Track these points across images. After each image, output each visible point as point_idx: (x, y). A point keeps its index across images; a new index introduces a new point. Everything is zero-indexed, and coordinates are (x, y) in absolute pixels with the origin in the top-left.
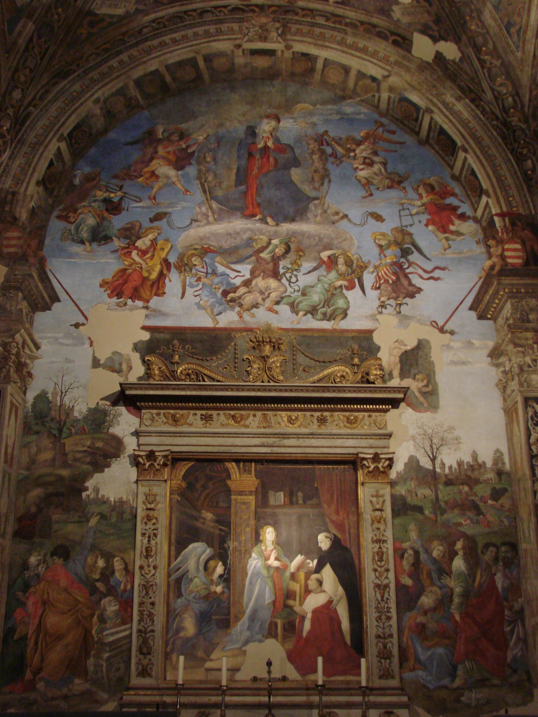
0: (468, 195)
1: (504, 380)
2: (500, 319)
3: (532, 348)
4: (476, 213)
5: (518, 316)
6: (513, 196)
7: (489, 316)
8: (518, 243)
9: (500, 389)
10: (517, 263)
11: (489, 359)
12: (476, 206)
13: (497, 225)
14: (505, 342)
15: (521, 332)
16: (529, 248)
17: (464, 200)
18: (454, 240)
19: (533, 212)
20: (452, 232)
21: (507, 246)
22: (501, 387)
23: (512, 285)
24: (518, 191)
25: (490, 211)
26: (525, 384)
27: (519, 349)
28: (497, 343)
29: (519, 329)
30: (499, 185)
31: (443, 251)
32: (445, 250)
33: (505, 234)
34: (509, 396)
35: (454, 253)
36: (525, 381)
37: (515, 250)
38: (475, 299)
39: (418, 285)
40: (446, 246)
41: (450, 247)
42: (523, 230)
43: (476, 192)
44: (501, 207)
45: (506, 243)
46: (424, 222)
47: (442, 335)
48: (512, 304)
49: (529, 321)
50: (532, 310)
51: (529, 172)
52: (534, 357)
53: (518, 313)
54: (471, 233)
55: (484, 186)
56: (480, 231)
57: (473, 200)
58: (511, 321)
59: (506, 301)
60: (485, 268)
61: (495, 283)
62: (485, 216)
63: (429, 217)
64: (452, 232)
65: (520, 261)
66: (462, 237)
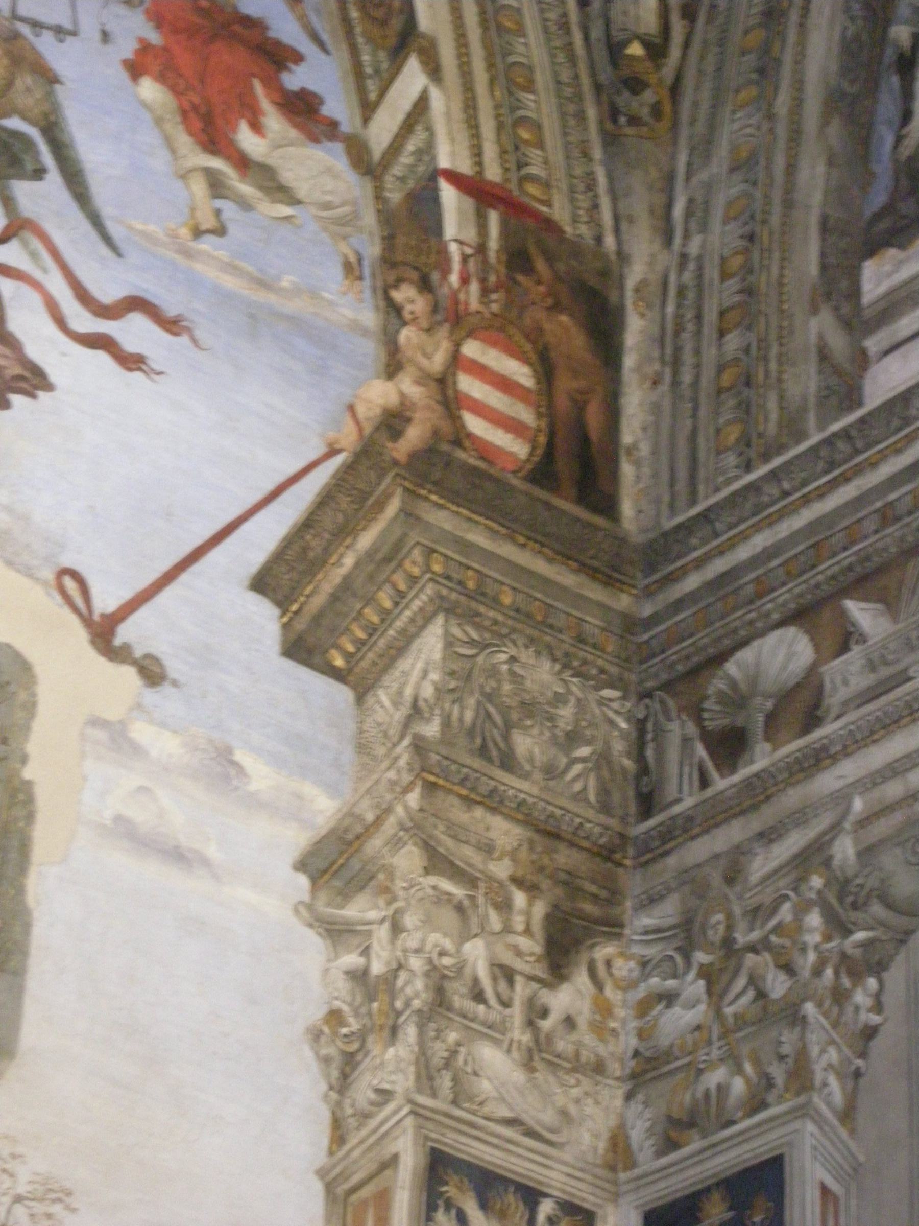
0: (346, 20)
1: (354, 1025)
2: (383, 696)
3: (504, 906)
4: (366, 120)
5: (469, 715)
6: (537, 127)
7: (339, 662)
8: (523, 358)
9: (326, 1060)
10: (499, 451)
11: (303, 881)
12: (372, 87)
13: (450, 230)
14: (390, 826)
15: (469, 802)
16: (562, 402)
17: (325, 37)
18: (245, 205)
19: (610, 241)
20: (243, 163)
21: (472, 349)
22: (331, 1051)
23: (466, 547)
24: (563, 115)
25: (428, 149)
26: (445, 1082)
27: (446, 885)
28: (351, 814)
29: (463, 782)
30: (487, 45)
31: (185, 232)
32: (198, 233)
33: (474, 287)
34: (367, 1116)
35: (230, 268)
36: (448, 1064)
37: (504, 384)
38: (288, 543)
39: (33, 351)
40: (208, 222)
41: (220, 231)
42: (556, 308)
43: (384, 23)
44: (477, 154)
45: (471, 334)
46: (127, 48)
47: (102, 660)
48: (449, 643)
49: (508, 762)
50: (529, 708)
51: (636, 49)
52: (508, 958)
53: (471, 702)
54: (327, 206)
55: (424, 22)
56: (369, 219)
57: (366, 58)
58: (431, 729)
59: (428, 619)
60: (361, 410)
61: (393, 507)
62: (405, 159)
63: (155, 37)
64: (243, 163)
65: (518, 448)
66: (286, 211)
